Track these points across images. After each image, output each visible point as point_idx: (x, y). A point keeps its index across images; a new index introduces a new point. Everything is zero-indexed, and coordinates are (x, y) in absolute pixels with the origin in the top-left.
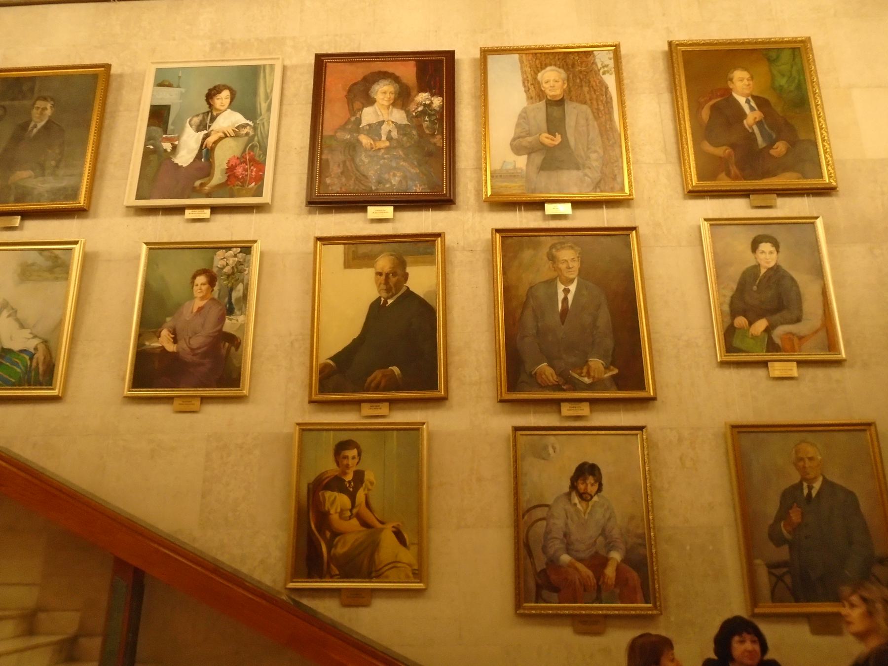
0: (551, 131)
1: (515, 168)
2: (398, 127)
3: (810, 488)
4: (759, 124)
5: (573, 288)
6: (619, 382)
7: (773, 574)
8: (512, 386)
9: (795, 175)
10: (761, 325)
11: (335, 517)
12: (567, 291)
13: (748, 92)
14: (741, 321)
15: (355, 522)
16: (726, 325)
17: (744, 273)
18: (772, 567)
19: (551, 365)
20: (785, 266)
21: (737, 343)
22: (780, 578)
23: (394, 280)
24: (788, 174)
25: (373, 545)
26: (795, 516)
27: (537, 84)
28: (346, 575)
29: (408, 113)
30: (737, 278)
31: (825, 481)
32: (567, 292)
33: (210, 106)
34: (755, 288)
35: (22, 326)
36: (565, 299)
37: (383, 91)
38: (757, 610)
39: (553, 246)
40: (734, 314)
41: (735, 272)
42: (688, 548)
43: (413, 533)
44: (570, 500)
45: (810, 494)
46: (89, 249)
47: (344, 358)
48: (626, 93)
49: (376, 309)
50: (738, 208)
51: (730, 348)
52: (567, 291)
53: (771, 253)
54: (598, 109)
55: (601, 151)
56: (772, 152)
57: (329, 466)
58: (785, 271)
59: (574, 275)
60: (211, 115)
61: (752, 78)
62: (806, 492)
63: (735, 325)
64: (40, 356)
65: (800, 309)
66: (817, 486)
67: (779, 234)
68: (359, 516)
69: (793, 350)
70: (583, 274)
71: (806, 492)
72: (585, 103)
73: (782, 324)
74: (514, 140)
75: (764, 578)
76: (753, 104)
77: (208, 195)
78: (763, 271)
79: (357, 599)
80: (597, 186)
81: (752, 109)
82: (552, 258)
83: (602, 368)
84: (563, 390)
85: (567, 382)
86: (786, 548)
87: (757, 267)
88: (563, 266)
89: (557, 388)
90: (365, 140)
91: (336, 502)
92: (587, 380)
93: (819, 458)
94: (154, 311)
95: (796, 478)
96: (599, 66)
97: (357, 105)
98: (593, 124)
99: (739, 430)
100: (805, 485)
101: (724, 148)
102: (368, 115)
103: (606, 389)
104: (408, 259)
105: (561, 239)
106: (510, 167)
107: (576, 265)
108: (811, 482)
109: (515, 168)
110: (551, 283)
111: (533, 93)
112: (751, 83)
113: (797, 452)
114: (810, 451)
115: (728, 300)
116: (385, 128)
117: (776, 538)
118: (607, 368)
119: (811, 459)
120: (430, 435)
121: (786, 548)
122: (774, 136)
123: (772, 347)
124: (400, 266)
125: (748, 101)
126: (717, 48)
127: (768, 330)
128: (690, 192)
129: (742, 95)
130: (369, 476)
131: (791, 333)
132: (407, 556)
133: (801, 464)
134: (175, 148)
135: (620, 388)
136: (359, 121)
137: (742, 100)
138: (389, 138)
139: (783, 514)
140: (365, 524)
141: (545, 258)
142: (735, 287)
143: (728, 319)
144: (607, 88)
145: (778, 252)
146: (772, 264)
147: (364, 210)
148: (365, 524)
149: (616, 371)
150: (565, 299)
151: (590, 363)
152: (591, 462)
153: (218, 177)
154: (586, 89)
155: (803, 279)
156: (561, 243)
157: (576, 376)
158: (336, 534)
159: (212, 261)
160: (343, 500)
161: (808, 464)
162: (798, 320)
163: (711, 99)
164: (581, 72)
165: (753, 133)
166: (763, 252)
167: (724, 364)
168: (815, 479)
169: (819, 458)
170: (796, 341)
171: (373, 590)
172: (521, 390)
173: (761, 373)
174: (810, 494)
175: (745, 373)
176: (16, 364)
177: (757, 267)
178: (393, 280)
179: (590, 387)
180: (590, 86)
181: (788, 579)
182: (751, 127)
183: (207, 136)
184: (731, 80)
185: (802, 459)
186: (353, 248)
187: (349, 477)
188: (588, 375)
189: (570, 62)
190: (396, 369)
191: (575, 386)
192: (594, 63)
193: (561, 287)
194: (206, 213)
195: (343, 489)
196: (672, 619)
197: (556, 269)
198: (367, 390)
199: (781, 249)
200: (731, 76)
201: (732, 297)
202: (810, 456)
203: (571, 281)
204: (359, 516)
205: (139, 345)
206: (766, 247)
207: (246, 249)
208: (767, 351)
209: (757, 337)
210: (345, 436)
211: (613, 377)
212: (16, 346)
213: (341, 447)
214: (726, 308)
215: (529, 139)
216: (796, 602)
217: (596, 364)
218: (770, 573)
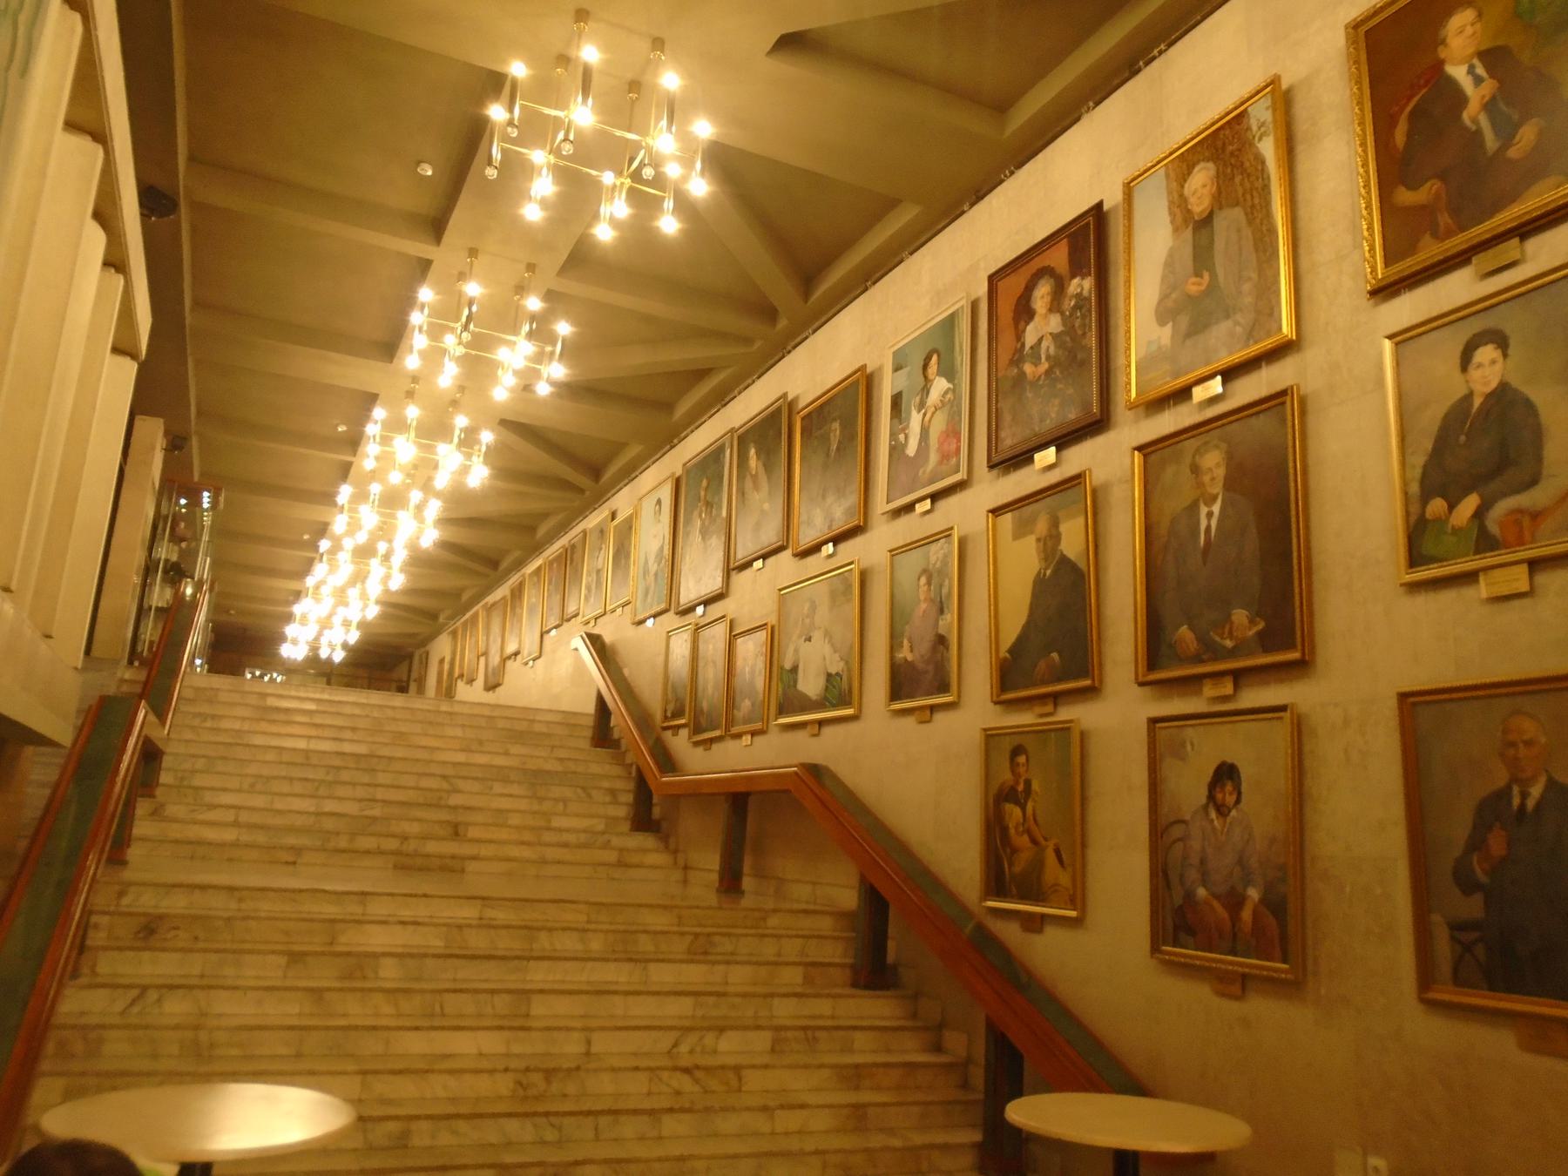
0: (1198, 274)
1: (1160, 348)
2: (1055, 337)
3: (1524, 795)
4: (1489, 106)
5: (1216, 508)
6: (1267, 641)
7: (1460, 942)
8: (1152, 665)
9: (1552, 180)
10: (1470, 503)
11: (1012, 831)
12: (1210, 515)
13: (1471, 50)
14: (1437, 506)
15: (1026, 838)
16: (1413, 519)
17: (1447, 416)
18: (1457, 927)
19: (1192, 628)
20: (1516, 382)
21: (1428, 547)
22: (1468, 948)
24: (1536, 188)
25: (1038, 865)
26: (1497, 843)
27: (1183, 199)
28: (1023, 898)
29: (1062, 314)
30: (1434, 428)
31: (1552, 784)
32: (1210, 516)
33: (926, 377)
34: (1463, 438)
36: (1208, 528)
37: (1042, 294)
38: (1431, 995)
39: (1197, 451)
40: (1425, 498)
41: (1430, 419)
42: (1348, 889)
43: (1075, 852)
44: (1207, 814)
45: (1523, 805)
46: (865, 564)
47: (1017, 649)
48: (1300, 149)
50: (1459, 288)
51: (1415, 558)
52: (1210, 515)
53: (1493, 362)
54: (1253, 206)
55: (1254, 276)
56: (1513, 153)
57: (1007, 776)
58: (1516, 391)
59: (1217, 489)
60: (926, 390)
61: (1480, 15)
62: (1516, 801)
63: (1428, 515)
65: (1539, 459)
66: (1536, 791)
67: (1510, 320)
68: (1028, 832)
69: (1521, 542)
70: (1230, 484)
71: (1516, 801)
72: (1237, 204)
73: (1504, 495)
74: (1159, 303)
75: (1443, 948)
76: (1480, 71)
78: (1477, 402)
79: (1034, 924)
80: (1250, 336)
81: (1478, 80)
82: (1195, 469)
83: (1246, 621)
84: (1202, 661)
85: (1210, 651)
86: (1477, 900)
87: (1469, 396)
88: (1206, 479)
89: (1197, 659)
90: (1028, 368)
91: (1013, 813)
92: (1229, 643)
93: (1543, 740)
95: (1500, 778)
96: (1255, 128)
97: (1022, 323)
98: (1247, 232)
99: (1409, 702)
100: (1516, 790)
101: (1429, 184)
102: (1031, 335)
103: (1251, 654)
104: (1060, 514)
105: (1205, 438)
106: (1154, 348)
107: (1220, 472)
108: (1525, 784)
109: (1160, 348)
110: (1193, 508)
111: (1179, 219)
112: (1478, 26)
113: (1505, 732)
114: (1529, 728)
115: (1418, 472)
116: (1044, 344)
117: (1467, 884)
118: (1252, 622)
119: (1529, 743)
120: (1082, 734)
121: (1477, 900)
122: (1516, 117)
123: (1485, 542)
125: (1471, 70)
126: (1377, 20)
127: (1479, 514)
128: (1374, 293)
129: (1460, 63)
130: (1035, 786)
131: (1520, 511)
132: (1064, 879)
133: (1512, 752)
134: (906, 437)
135: (1267, 650)
136: (1023, 345)
137: (1458, 72)
138: (1048, 358)
139: (1476, 843)
140: (1034, 841)
141: (1188, 470)
142: (1429, 445)
143: (1415, 508)
144: (1263, 163)
145: (1505, 355)
146: (1494, 384)
147: (1031, 460)
148: (1034, 841)
149: (1261, 625)
150: (1208, 528)
151: (1234, 618)
152: (1229, 761)
153: (933, 457)
154: (1238, 179)
156: (1206, 443)
157: (1217, 639)
158: (1015, 851)
160: (1017, 811)
161: (1522, 751)
162: (1534, 482)
163: (1410, 99)
164: (1232, 154)
165: (1478, 133)
166: (1480, 365)
167: (1415, 587)
168: (1533, 779)
169: (1543, 740)
170: (1526, 521)
171: (1043, 916)
172: (1161, 668)
173: (1468, 593)
174: (1523, 805)
175: (1448, 597)
177: (1469, 396)
178: (1049, 543)
179: (1232, 653)
180: (1244, 171)
181: (1480, 950)
182: (1475, 121)
184: (1443, 42)
185: (1513, 744)
186: (1016, 513)
187: (1021, 788)
188: (1231, 636)
189: (1219, 144)
190: (1055, 655)
191: (1216, 653)
192: (1249, 129)
193: (1204, 510)
194: (927, 504)
195: (1017, 803)
196: (1323, 991)
197: (1200, 485)
198: (1034, 685)
199: (1510, 351)
200: (1443, 33)
201: (1425, 467)
202: (1525, 738)
203: (1214, 498)
204: (1028, 832)
205: (892, 658)
206: (1486, 353)
208: (1477, 552)
209: (1461, 529)
210: (1016, 741)
211: (1260, 634)
213: (1017, 751)
214: (1415, 488)
215: (1174, 296)
216: (1491, 989)
217: (1240, 616)
218: (1452, 938)
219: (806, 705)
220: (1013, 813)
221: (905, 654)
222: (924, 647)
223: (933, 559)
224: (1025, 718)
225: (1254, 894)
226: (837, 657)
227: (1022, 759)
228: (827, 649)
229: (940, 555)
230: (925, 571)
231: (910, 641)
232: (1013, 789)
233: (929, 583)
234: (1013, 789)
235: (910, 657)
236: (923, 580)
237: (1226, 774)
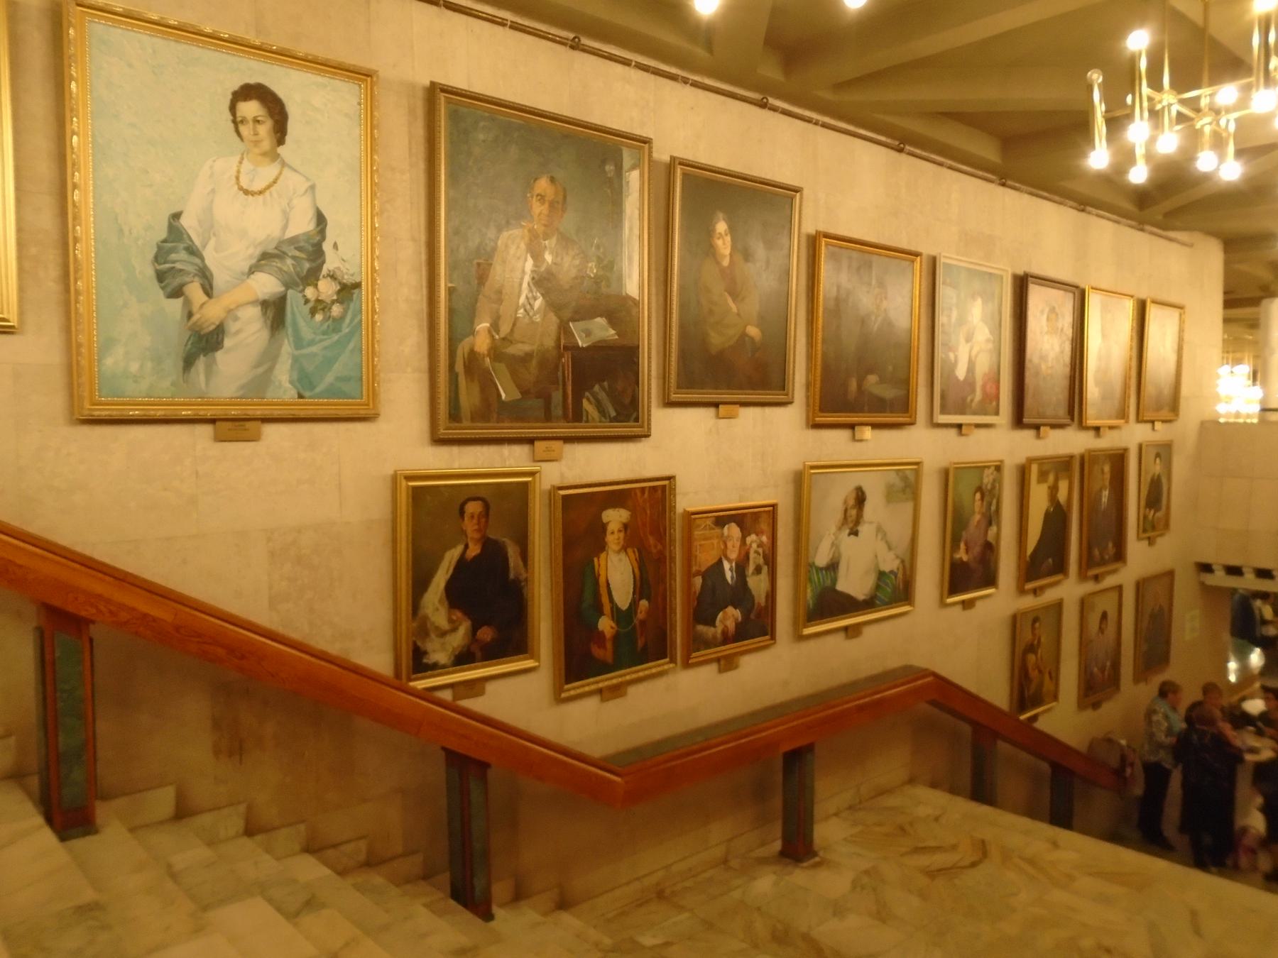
23: (1054, 490)
32: (1106, 494)
35: (890, 548)
49: (1047, 514)
51: (1145, 531)
59: (1107, 483)
64: (900, 576)
77: (975, 413)
90: (1043, 367)
91: (1031, 658)
94: (955, 525)
110: (1101, 491)
124: (1057, 480)
130: (1043, 640)
140: (1040, 672)
155: (1164, 480)
159: (982, 479)
176: (887, 584)
183: (971, 349)
207: (998, 468)
212: (886, 568)
219: (847, 605)
220: (1031, 658)
221: (962, 555)
222: (977, 550)
223: (985, 480)
224: (1028, 602)
225: (1108, 664)
226: (891, 555)
227: (1037, 625)
228: (881, 547)
229: (991, 478)
230: (979, 489)
231: (966, 544)
232: (1032, 645)
233: (982, 499)
234: (1032, 645)
235: (965, 558)
236: (978, 496)
237: (1104, 616)
